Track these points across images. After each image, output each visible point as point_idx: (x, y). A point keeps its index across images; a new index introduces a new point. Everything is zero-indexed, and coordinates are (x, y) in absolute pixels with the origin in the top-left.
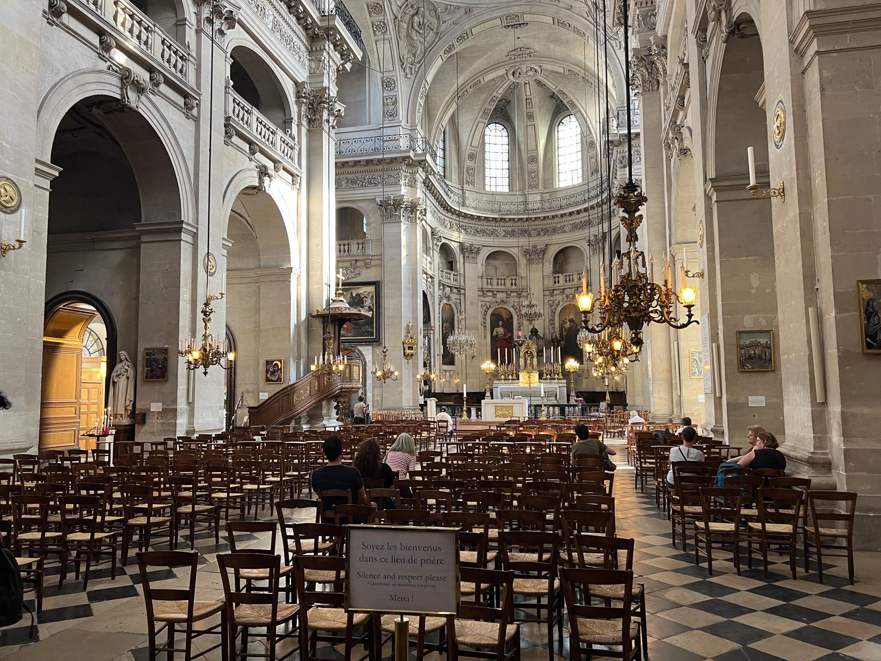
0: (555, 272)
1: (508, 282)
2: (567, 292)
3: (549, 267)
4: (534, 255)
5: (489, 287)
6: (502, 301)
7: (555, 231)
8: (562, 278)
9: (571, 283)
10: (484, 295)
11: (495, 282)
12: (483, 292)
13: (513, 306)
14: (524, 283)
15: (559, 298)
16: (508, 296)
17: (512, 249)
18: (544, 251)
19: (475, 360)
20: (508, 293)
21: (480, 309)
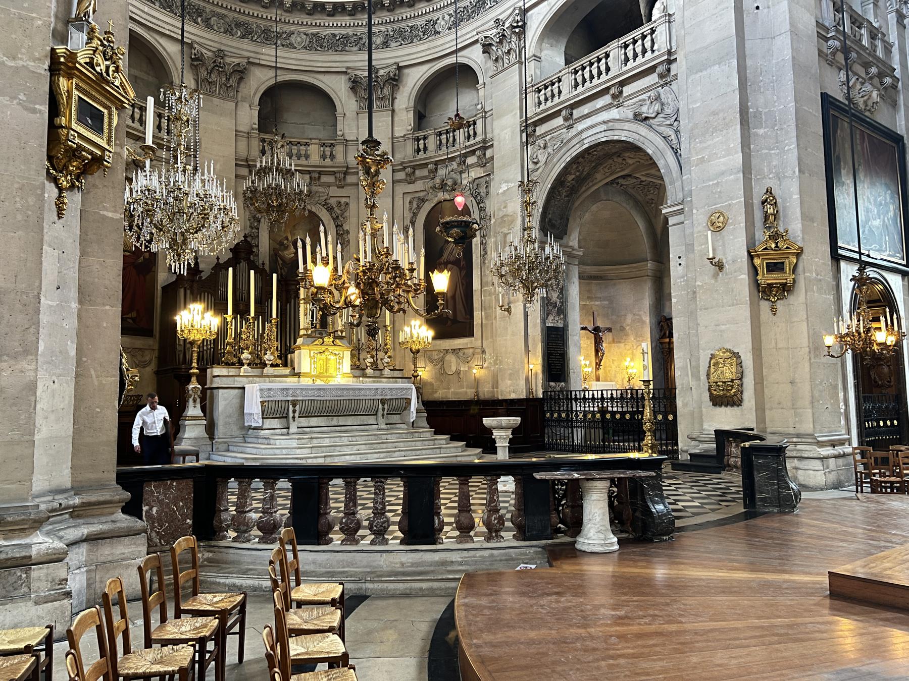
3: (249, 116)
4: (218, 76)
7: (268, 37)
9: (303, 161)
17: (163, 41)
18: (241, 73)
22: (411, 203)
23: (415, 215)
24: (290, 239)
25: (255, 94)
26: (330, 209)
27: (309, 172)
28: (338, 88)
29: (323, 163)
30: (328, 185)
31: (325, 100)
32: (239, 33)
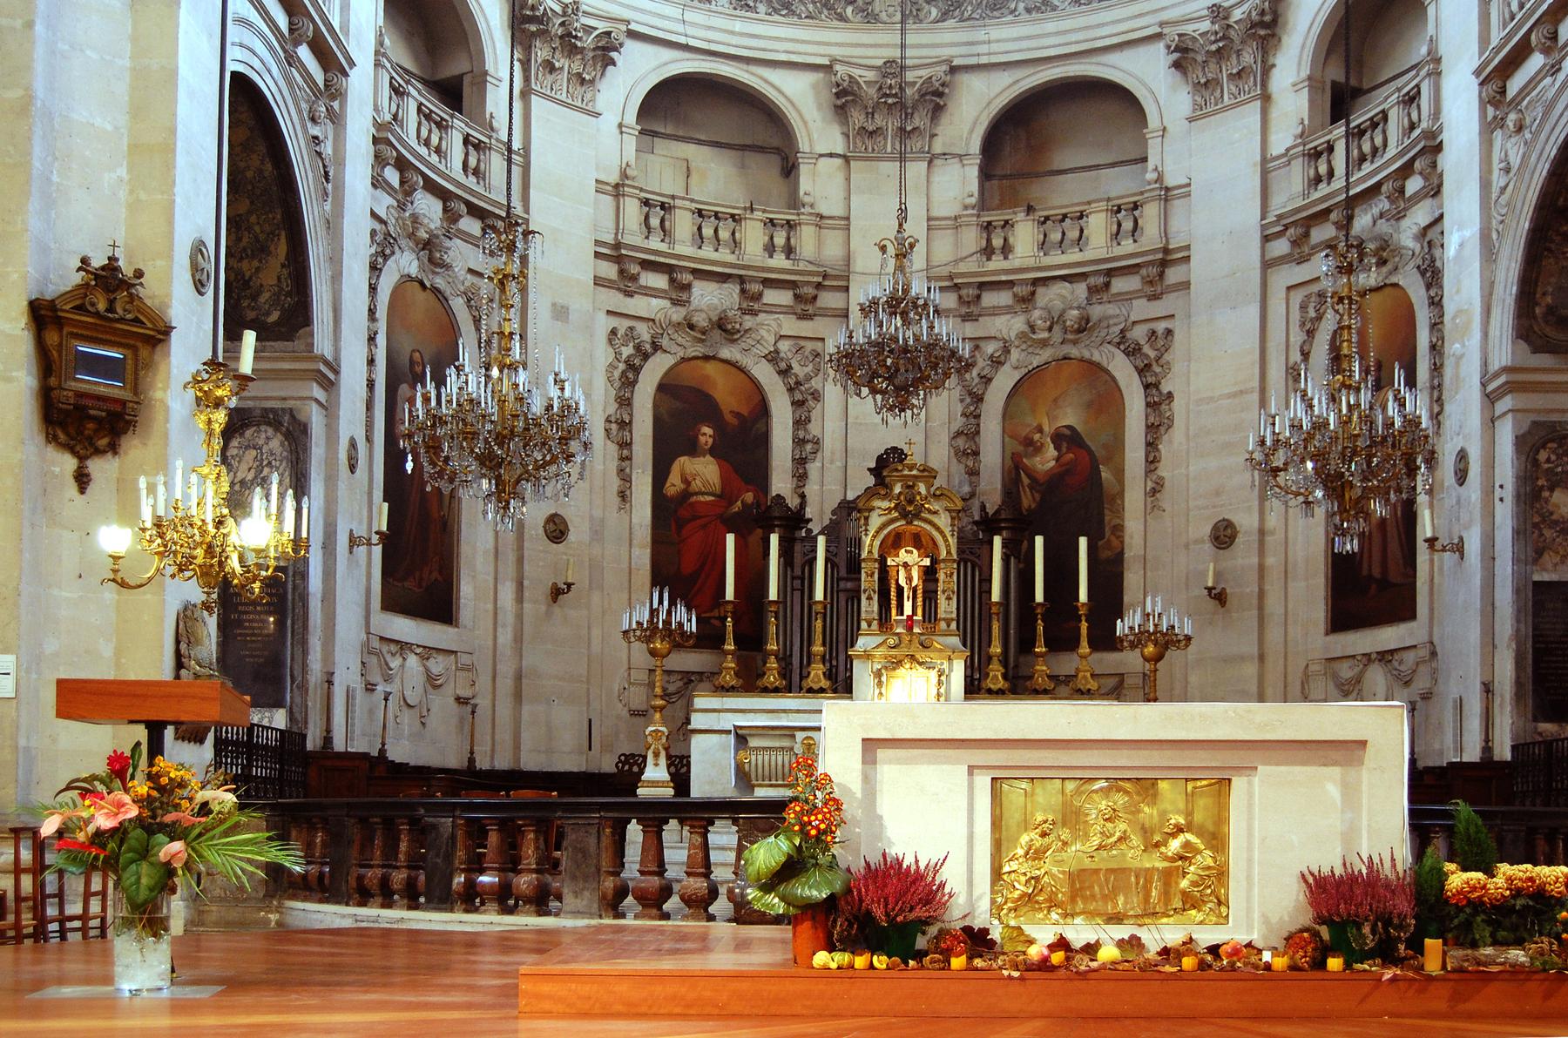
0: (983, 204)
1: (753, 236)
2: (1051, 297)
3: (957, 184)
4: (889, 112)
5: (655, 243)
6: (723, 327)
8: (1025, 237)
9: (1074, 256)
10: (627, 283)
11: (683, 224)
12: (622, 266)
13: (773, 358)
14: (832, 250)
15: (1011, 326)
16: (751, 301)
17: (775, 76)
18: (935, 99)
19: (569, 608)
20: (750, 287)
21: (603, 355)
22: (1303, 307)
23: (1310, 333)
24: (1046, 429)
25: (971, 131)
26: (1133, 351)
27: (1084, 276)
28: (1147, 73)
29: (1118, 251)
30: (1127, 297)
31: (1116, 100)
32: (934, 12)
